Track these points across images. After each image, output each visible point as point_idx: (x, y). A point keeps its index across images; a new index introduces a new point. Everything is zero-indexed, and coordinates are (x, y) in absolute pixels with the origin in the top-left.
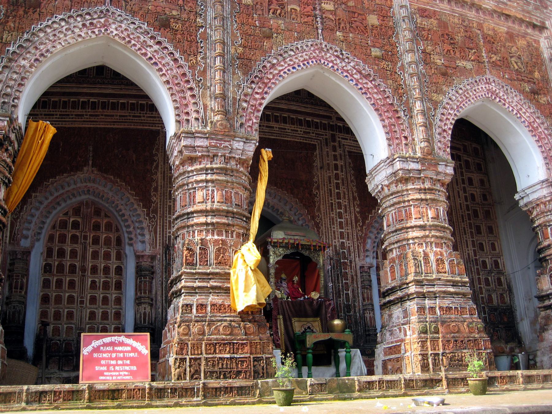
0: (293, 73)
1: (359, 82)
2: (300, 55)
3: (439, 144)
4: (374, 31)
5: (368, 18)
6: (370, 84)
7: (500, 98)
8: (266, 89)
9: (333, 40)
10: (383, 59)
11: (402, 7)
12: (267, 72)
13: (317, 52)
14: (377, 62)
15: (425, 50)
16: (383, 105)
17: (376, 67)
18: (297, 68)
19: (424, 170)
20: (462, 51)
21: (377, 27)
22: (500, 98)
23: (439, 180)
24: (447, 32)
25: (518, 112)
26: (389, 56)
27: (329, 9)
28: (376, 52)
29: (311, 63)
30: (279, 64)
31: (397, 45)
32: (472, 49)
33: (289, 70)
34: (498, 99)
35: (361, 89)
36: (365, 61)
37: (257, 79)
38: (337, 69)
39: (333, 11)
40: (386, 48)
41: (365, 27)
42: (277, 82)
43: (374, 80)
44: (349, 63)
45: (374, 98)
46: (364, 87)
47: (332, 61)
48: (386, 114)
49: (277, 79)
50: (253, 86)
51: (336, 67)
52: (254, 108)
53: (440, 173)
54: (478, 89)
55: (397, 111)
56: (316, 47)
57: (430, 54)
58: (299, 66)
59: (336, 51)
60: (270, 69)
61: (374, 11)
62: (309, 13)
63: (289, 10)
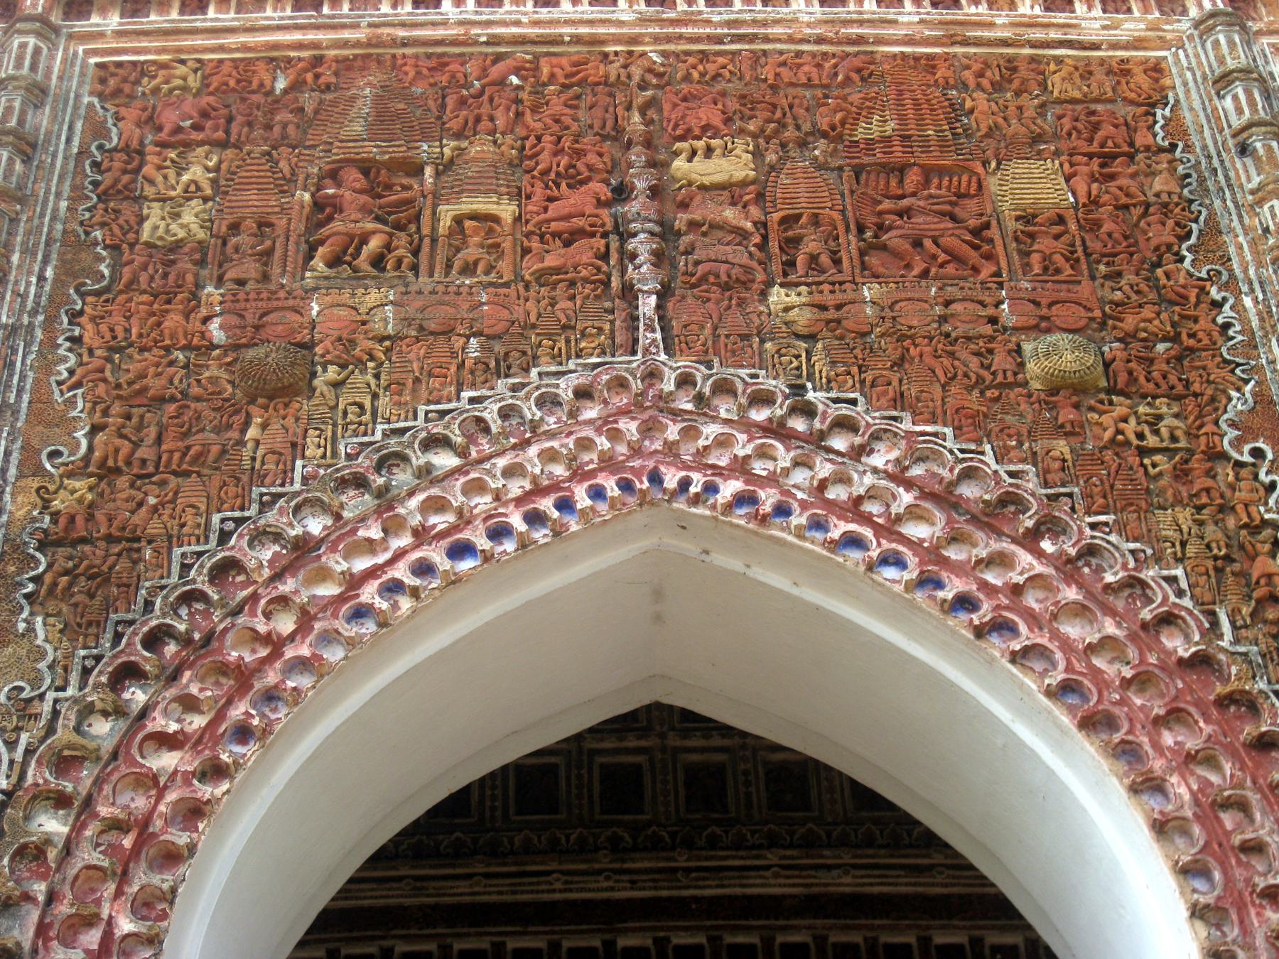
0: (454, 581)
1: (945, 562)
2: (501, 462)
4: (1044, 244)
5: (992, 183)
6: (1025, 558)
8: (238, 711)
9: (744, 343)
10: (1110, 391)
11: (1223, 81)
12: (254, 597)
13: (630, 427)
14: (1067, 415)
16: (1141, 681)
17: (1062, 447)
18: (483, 543)
21: (1061, 220)
26: (1161, 366)
27: (718, 178)
28: (1055, 355)
29: (582, 499)
30: (343, 535)
31: (1215, 293)
33: (424, 569)
35: (964, 603)
36: (972, 425)
37: (171, 649)
38: (782, 510)
39: (744, 183)
40: (1130, 322)
41: (976, 232)
42: (334, 655)
43: (1049, 526)
44: (858, 452)
45: (1066, 645)
46: (984, 585)
47: (740, 467)
48: (1168, 739)
49: (329, 637)
50: (137, 696)
51: (768, 498)
52: (127, 842)
56: (622, 400)
58: (499, 533)
59: (762, 399)
60: (277, 577)
61: (1037, 139)
62: (579, 222)
63: (445, 223)
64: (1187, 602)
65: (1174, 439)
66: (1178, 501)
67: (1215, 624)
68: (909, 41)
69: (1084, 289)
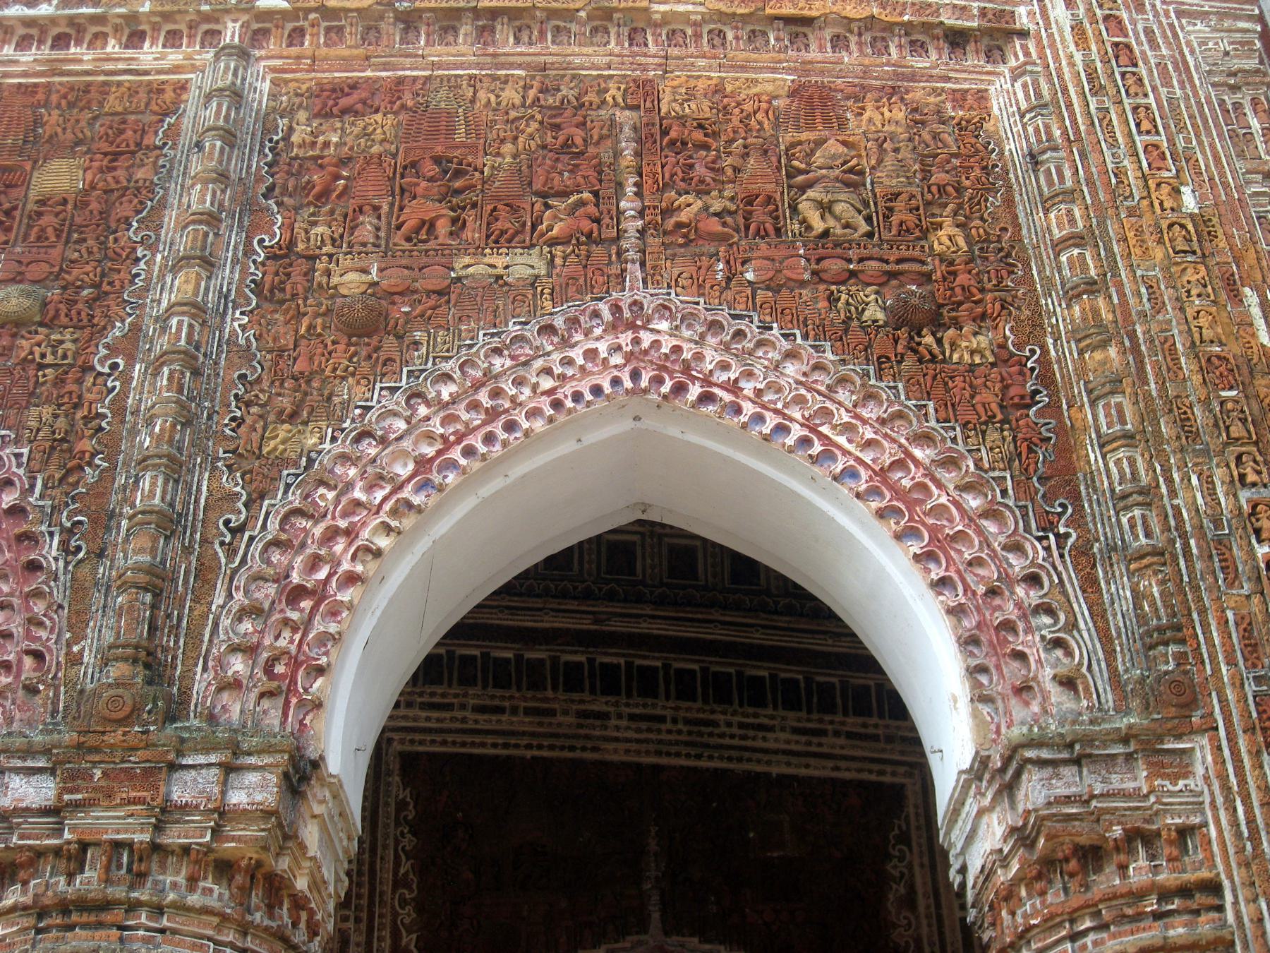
3: (238, 665)
7: (707, 381)
10: (41, 324)
15: (292, 243)
19: (77, 805)
20: (503, 212)
21: (65, 202)
22: (707, 381)
23: (186, 850)
24: (439, 149)
25: (813, 430)
26: (80, 306)
32: (565, 194)
34: (695, 391)
53: (185, 808)
54: (568, 362)
55: (28, 538)
57: (313, 258)
64: (21, 472)
65: (65, 357)
66: (48, 401)
67: (32, 486)
68: (25, 74)
69: (55, 253)
